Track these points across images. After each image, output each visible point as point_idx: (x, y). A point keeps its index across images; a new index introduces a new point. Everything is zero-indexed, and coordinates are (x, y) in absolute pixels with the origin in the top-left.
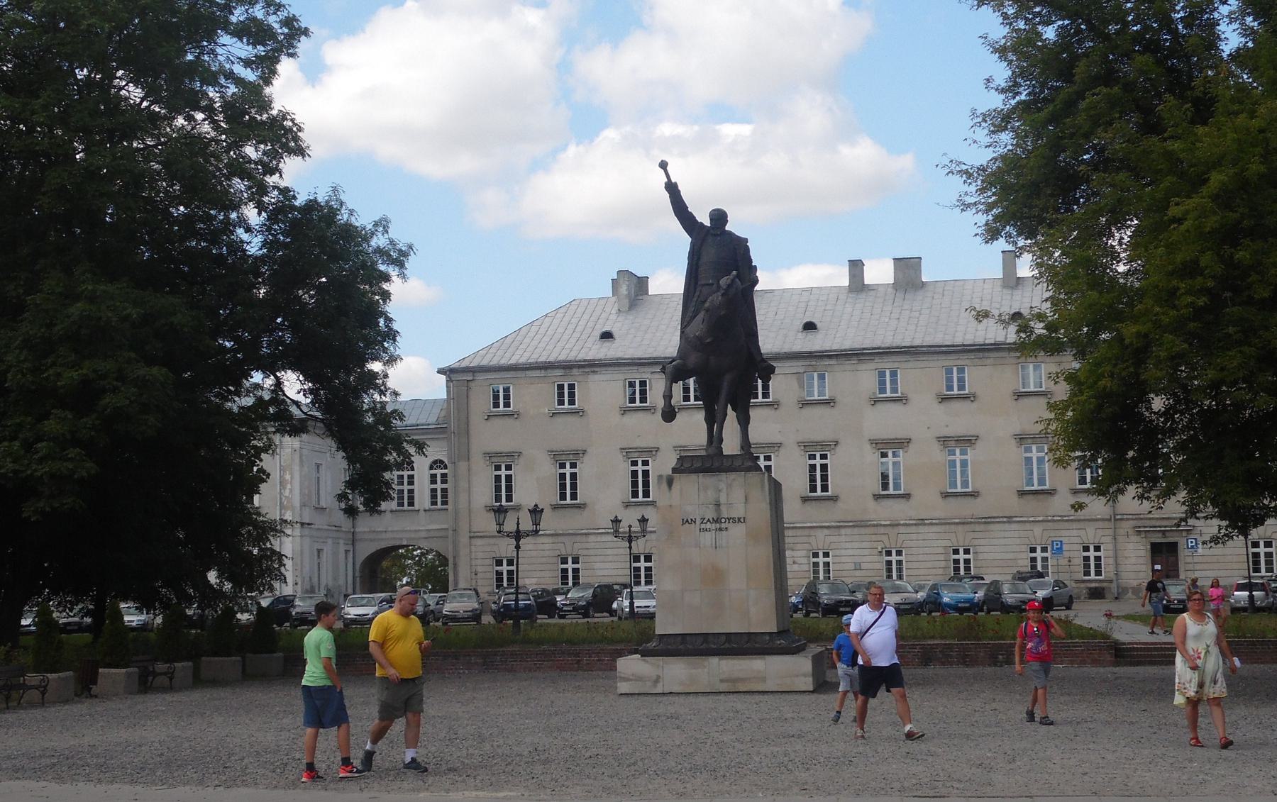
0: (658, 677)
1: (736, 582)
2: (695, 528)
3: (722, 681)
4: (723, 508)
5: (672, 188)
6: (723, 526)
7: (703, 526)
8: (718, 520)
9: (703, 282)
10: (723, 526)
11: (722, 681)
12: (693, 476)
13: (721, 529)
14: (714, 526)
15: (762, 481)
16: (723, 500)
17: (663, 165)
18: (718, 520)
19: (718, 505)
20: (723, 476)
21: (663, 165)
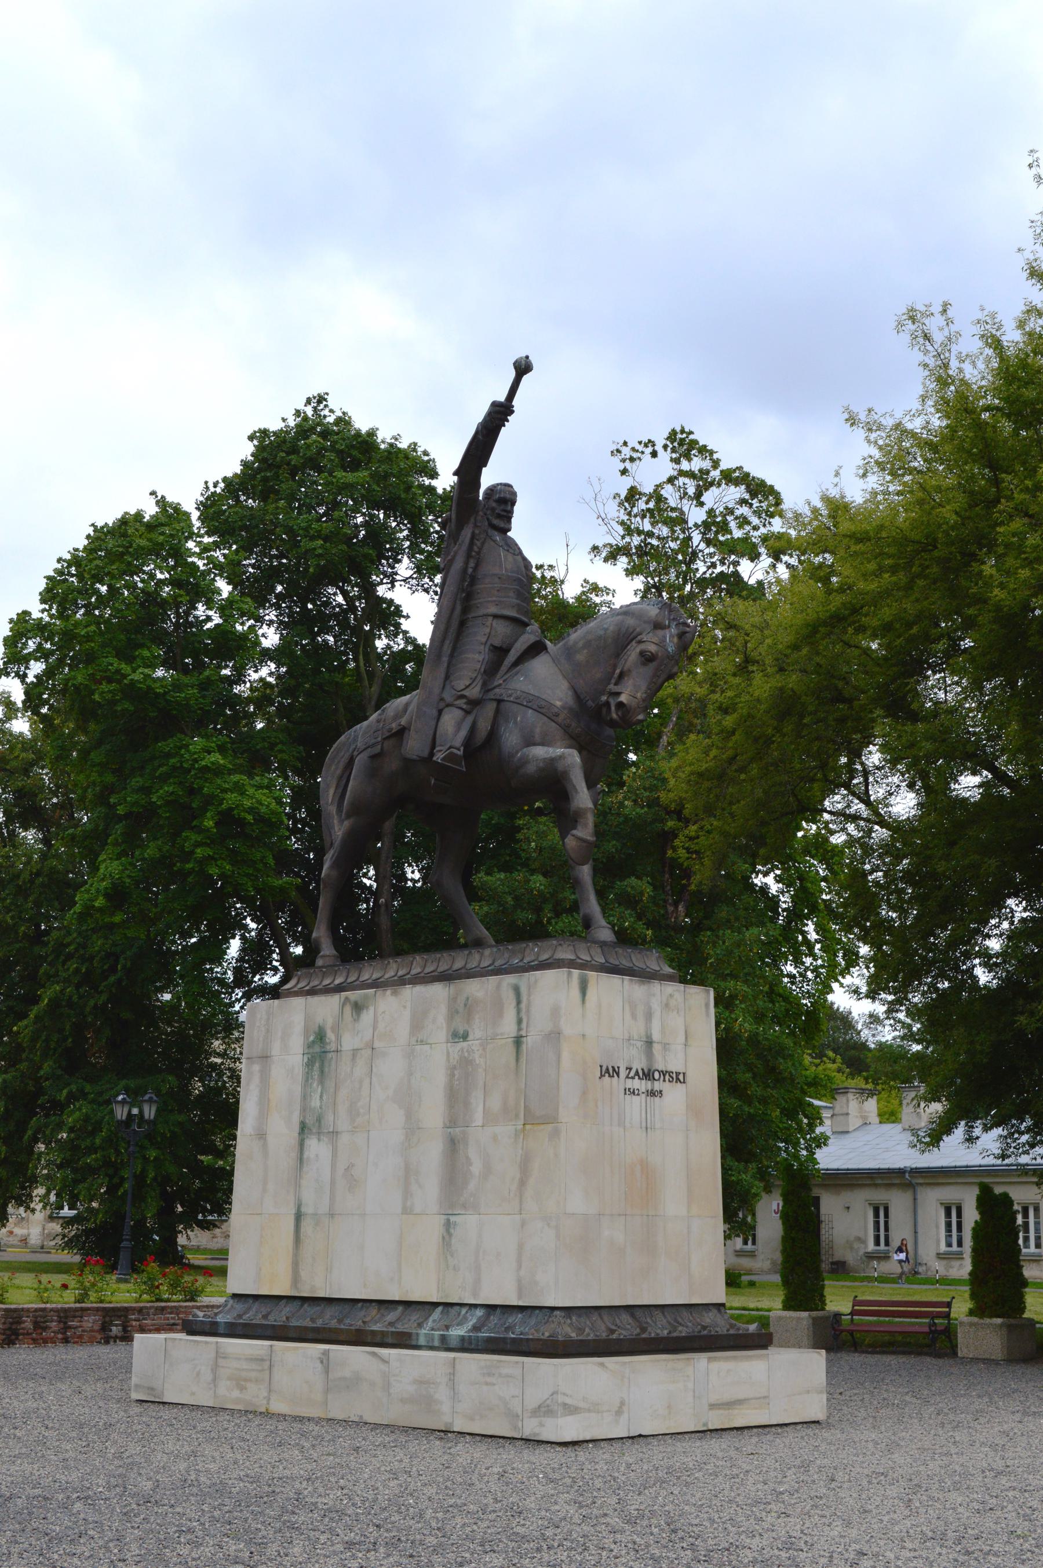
0: (622, 1403)
1: (673, 1203)
2: (617, 1084)
3: (713, 1406)
5: (500, 414)
7: (630, 1084)
8: (648, 1075)
9: (493, 610)
10: (657, 1086)
11: (713, 1406)
12: (616, 980)
13: (652, 1093)
15: (707, 1005)
16: (656, 1036)
17: (523, 368)
19: (649, 1043)
20: (656, 986)
21: (523, 368)
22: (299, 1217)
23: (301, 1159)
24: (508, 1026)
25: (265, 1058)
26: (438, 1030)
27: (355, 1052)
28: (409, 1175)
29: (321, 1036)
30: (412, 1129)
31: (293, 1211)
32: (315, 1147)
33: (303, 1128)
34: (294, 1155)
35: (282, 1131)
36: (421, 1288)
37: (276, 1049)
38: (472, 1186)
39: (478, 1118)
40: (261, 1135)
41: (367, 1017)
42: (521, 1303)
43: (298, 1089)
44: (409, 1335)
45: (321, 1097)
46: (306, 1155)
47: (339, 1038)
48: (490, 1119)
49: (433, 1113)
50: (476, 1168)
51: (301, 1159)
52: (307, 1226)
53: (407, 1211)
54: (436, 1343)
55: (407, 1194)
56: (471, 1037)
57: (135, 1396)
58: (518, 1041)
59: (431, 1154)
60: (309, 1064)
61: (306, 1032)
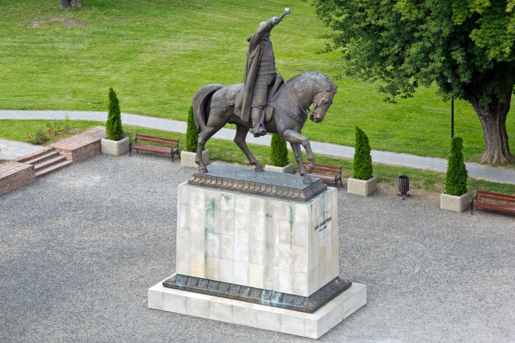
4: (326, 214)
6: (325, 225)
13: (325, 228)
14: (322, 227)
18: (324, 223)
22: (206, 256)
23: (206, 239)
24: (287, 217)
25: (188, 204)
26: (261, 213)
27: (227, 212)
28: (251, 253)
29: (213, 204)
30: (252, 239)
32: (211, 236)
33: (206, 230)
34: (203, 237)
35: (197, 229)
36: (256, 282)
37: (192, 203)
38: (275, 259)
39: (277, 241)
40: (188, 228)
41: (232, 201)
43: (203, 218)
44: (258, 301)
45: (213, 222)
46: (208, 238)
47: (220, 205)
48: (281, 242)
49: (260, 237)
50: (277, 254)
51: (206, 239)
52: (209, 260)
54: (268, 304)
55: (250, 258)
56: (273, 217)
57: (150, 306)
58: (291, 222)
59: (260, 248)
60: (208, 211)
61: (206, 200)
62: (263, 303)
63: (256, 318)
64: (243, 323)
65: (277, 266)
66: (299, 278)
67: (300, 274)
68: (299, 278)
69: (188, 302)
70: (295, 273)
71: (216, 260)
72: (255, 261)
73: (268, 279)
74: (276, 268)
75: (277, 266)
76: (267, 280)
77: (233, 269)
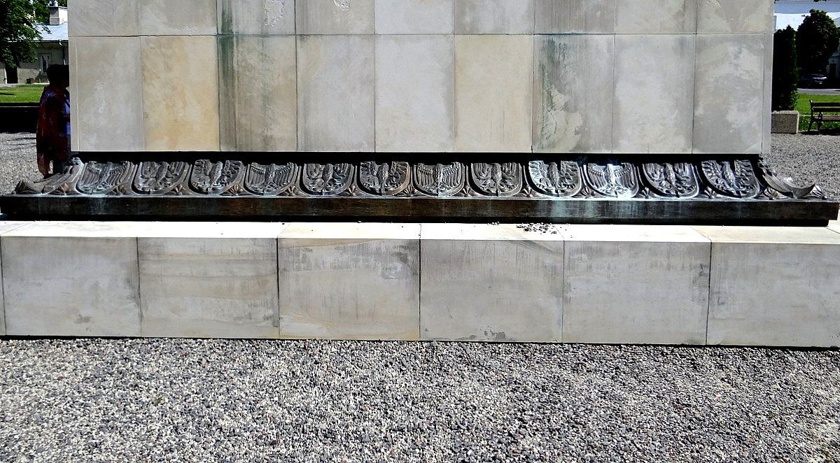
22: (226, 41)
31: (212, 30)
42: (695, 152)
52: (244, 55)
53: (463, 28)
62: (559, 212)
63: (562, 292)
64: (483, 326)
65: (606, 26)
66: (725, 69)
67: (732, 49)
68: (725, 69)
69: (150, 267)
70: (700, 47)
71: (282, 48)
72: (488, 26)
73: (560, 99)
74: (600, 41)
75: (606, 26)
76: (552, 105)
77: (370, 82)
